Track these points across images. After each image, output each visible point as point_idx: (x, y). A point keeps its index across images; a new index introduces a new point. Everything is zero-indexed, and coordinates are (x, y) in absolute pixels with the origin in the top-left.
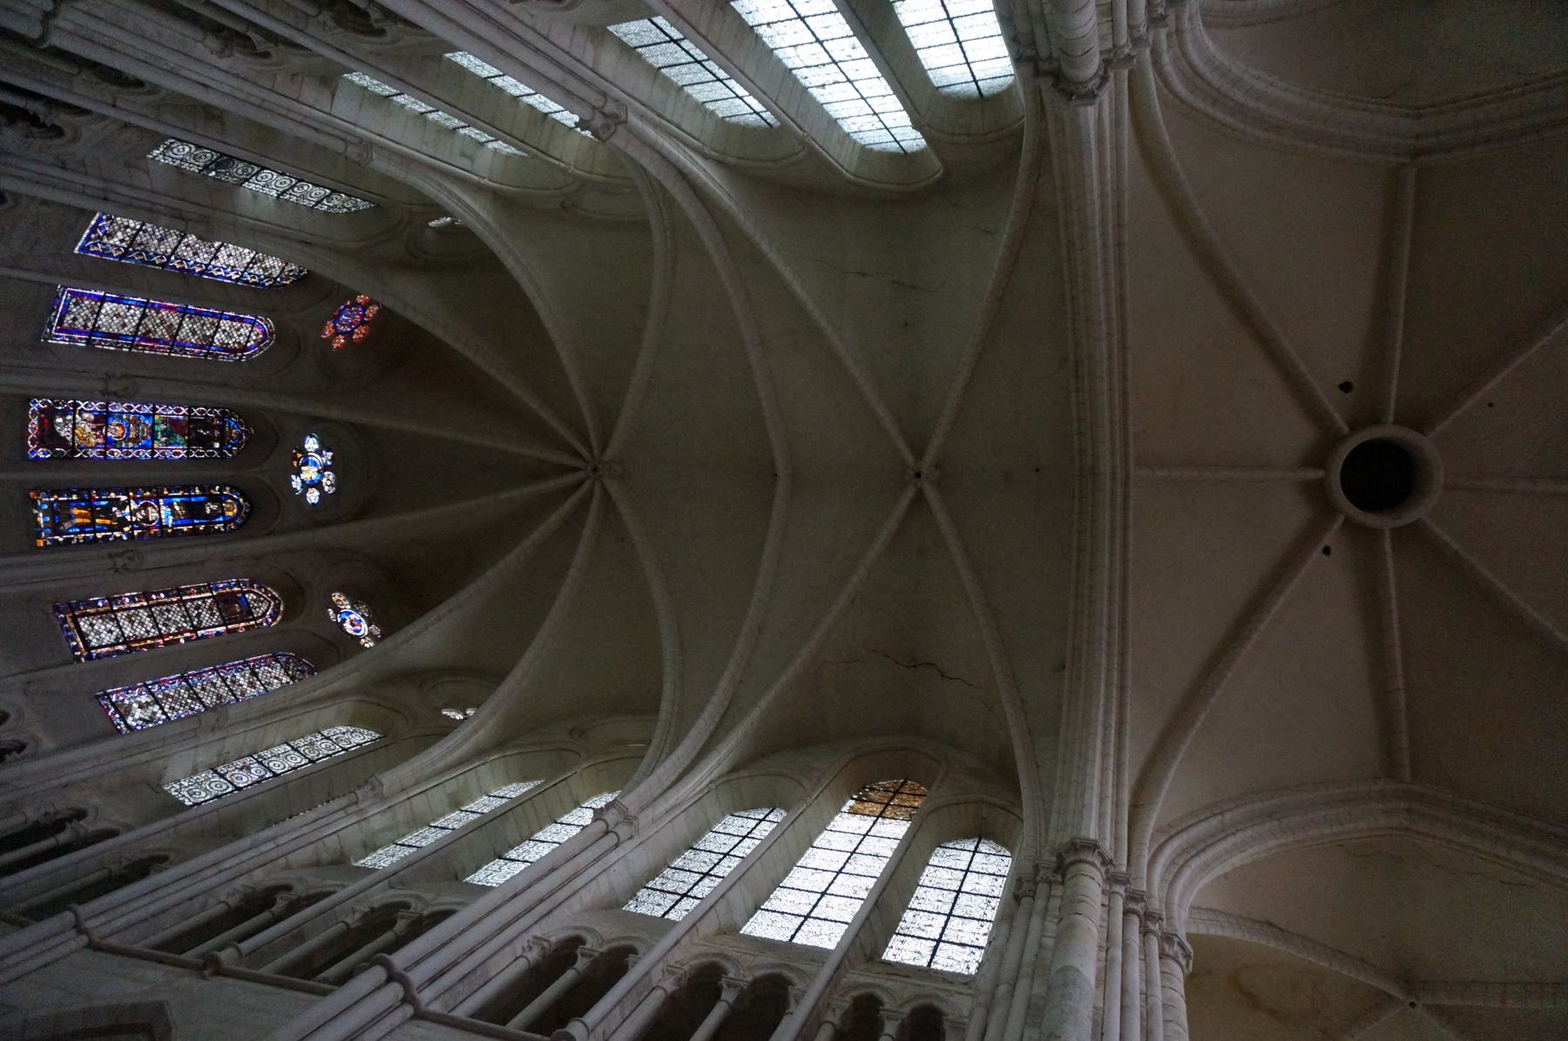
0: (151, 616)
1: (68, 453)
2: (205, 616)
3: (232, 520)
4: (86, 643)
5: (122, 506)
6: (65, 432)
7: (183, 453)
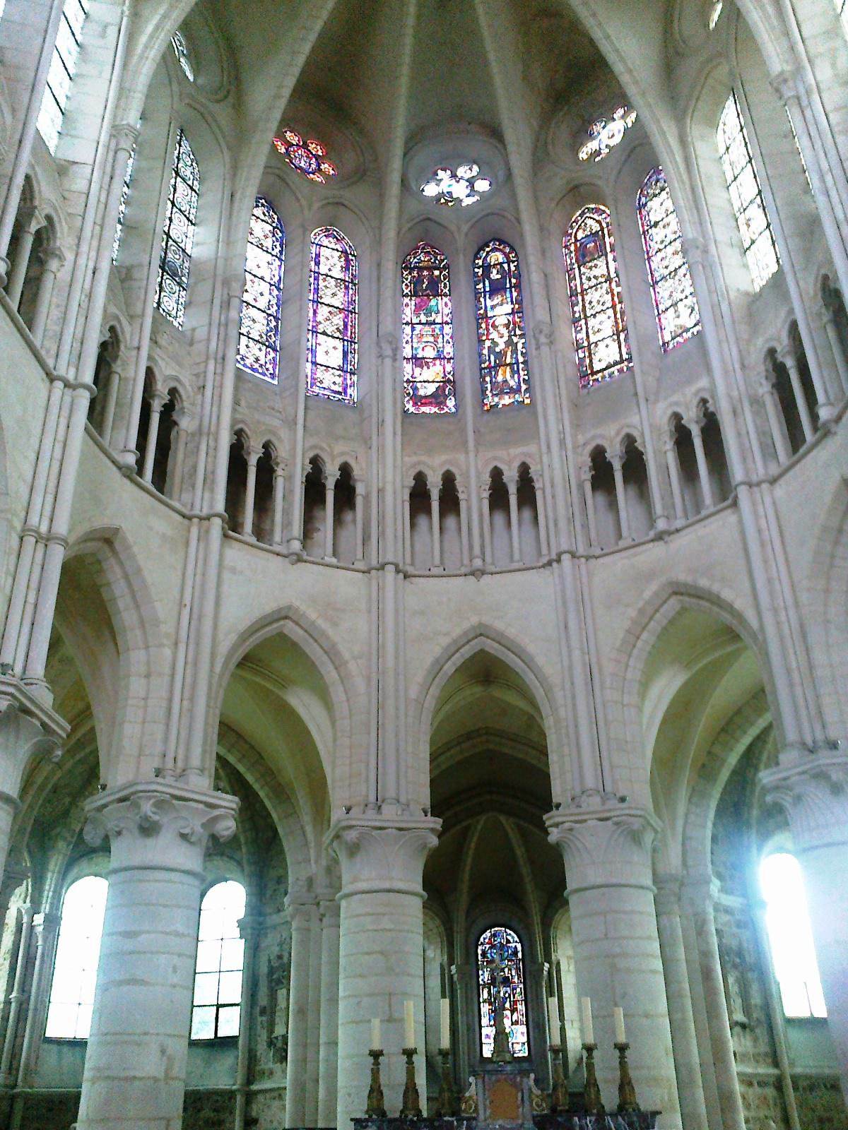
1: (448, 385)
2: (596, 272)
3: (506, 255)
4: (616, 363)
5: (495, 344)
6: (431, 389)
7: (445, 299)
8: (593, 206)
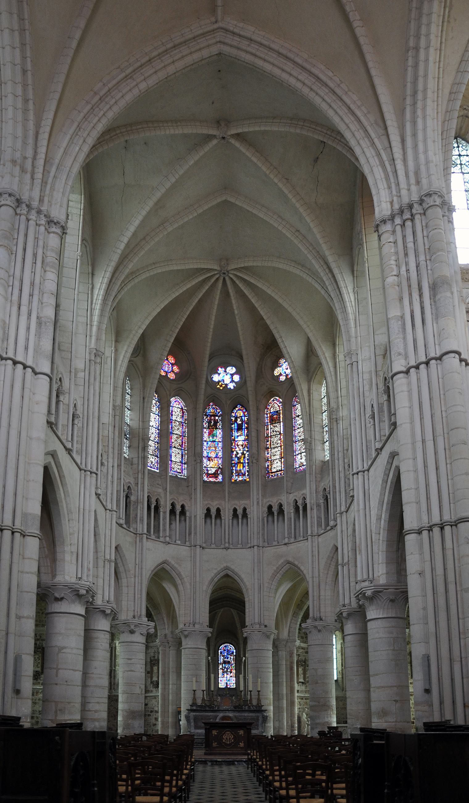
0: (274, 448)
2: (276, 429)
3: (244, 413)
4: (280, 471)
5: (238, 453)
8: (277, 398)
